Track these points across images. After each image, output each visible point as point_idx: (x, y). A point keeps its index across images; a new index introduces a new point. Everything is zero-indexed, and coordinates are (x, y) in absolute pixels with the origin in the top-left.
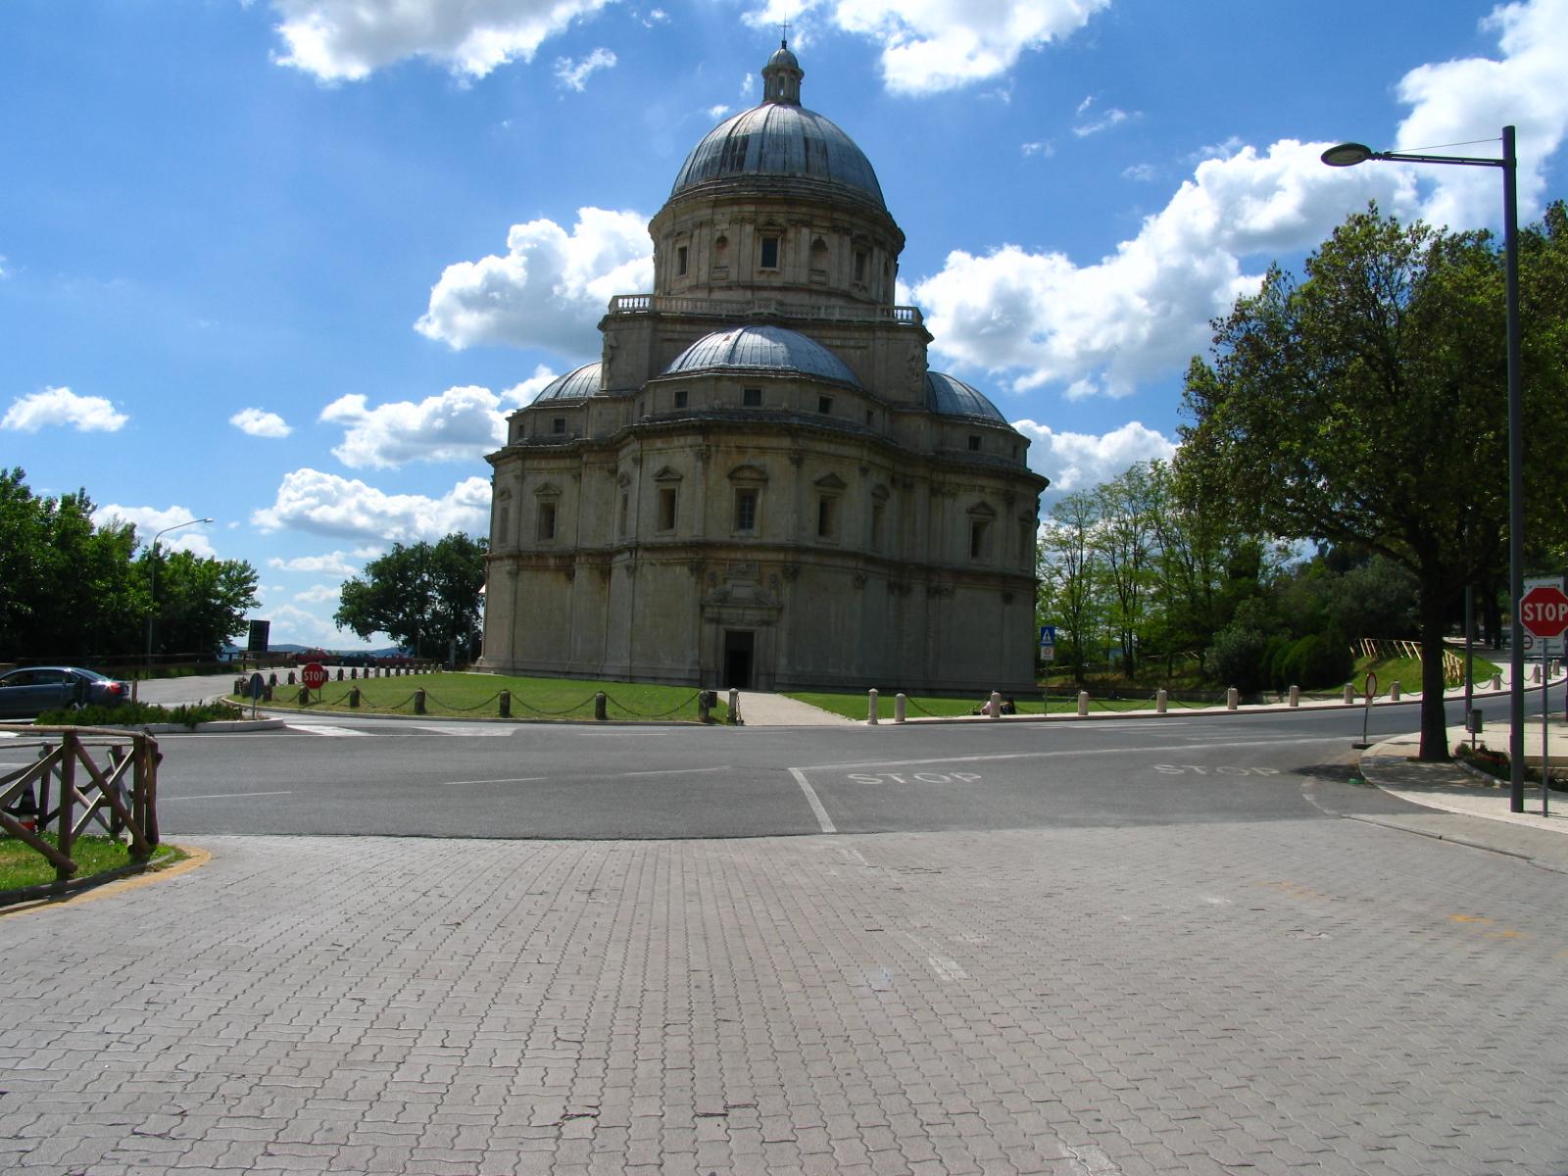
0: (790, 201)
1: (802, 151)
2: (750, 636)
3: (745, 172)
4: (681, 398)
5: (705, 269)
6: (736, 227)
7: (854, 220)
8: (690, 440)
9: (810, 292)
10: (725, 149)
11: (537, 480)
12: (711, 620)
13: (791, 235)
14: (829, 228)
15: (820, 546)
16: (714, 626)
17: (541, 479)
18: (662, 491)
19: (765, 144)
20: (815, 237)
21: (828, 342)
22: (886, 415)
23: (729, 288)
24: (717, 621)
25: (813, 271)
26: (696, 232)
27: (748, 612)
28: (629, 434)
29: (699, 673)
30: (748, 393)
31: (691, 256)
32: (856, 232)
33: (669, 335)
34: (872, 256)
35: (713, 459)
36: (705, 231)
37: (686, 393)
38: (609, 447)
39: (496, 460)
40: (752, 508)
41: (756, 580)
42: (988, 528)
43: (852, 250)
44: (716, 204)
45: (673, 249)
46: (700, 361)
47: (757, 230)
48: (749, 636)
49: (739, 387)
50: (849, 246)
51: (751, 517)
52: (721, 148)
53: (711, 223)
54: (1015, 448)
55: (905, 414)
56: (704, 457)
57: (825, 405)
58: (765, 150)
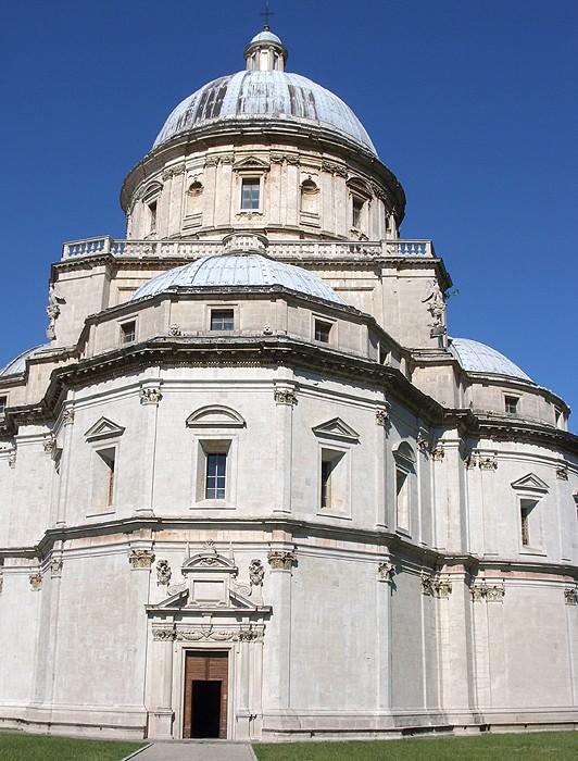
0: (270, 139)
1: (286, 94)
2: (223, 654)
3: (221, 117)
4: (128, 328)
12: (163, 635)
13: (276, 170)
16: (165, 644)
23: (204, 233)
27: (216, 620)
28: (59, 382)
30: (215, 314)
32: (350, 176)
33: (129, 284)
41: (231, 572)
44: (188, 150)
46: (154, 291)
48: (223, 654)
49: (204, 306)
51: (222, 483)
54: (557, 416)
55: (423, 365)
57: (323, 330)
58: (244, 96)
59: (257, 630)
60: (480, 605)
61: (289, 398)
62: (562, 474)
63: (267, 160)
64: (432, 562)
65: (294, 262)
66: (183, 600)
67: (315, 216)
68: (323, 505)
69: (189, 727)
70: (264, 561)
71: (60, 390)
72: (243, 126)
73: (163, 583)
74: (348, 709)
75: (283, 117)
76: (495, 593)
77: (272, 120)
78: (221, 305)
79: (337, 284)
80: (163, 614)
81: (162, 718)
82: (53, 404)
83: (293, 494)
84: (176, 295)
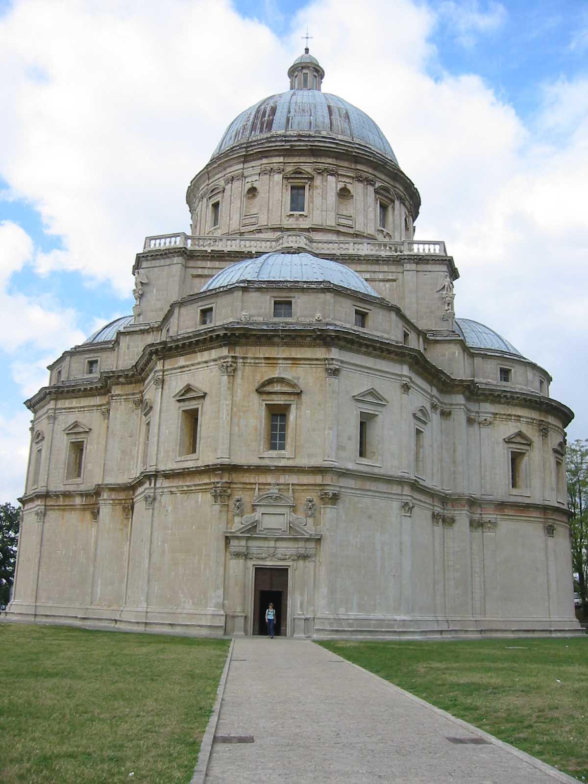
1: (326, 111)
2: (284, 571)
3: (273, 132)
4: (206, 313)
5: (236, 217)
7: (376, 173)
8: (214, 354)
9: (338, 233)
10: (256, 117)
11: (66, 420)
12: (237, 555)
13: (318, 181)
14: (353, 178)
15: (362, 468)
16: (241, 561)
17: (71, 419)
18: (185, 411)
19: (292, 110)
20: (341, 185)
22: (421, 339)
23: (259, 231)
24: (246, 556)
25: (339, 215)
26: (228, 187)
27: (280, 544)
28: (151, 354)
29: (223, 618)
31: (222, 208)
32: (377, 185)
33: (200, 272)
34: (393, 208)
35: (239, 373)
36: (237, 184)
37: (211, 309)
38: (137, 375)
39: (34, 405)
40: (283, 428)
42: (526, 458)
44: (246, 159)
45: (207, 206)
46: (227, 281)
47: (285, 178)
49: (268, 297)
50: (373, 195)
51: (283, 437)
52: (252, 117)
53: (243, 176)
54: (541, 382)
56: (230, 370)
58: (292, 114)
59: (312, 552)
60: (478, 534)
61: (335, 372)
63: (309, 170)
64: (445, 499)
65: (332, 257)
66: (254, 527)
67: (349, 217)
68: (362, 454)
69: (257, 627)
70: (316, 501)
71: (149, 360)
72: (291, 141)
73: (238, 515)
74: (379, 615)
75: (324, 133)
76: (489, 525)
77: (314, 137)
78: (283, 296)
79: (368, 276)
80: (238, 538)
81: (236, 619)
82: (143, 370)
83: (340, 448)
84: (246, 287)
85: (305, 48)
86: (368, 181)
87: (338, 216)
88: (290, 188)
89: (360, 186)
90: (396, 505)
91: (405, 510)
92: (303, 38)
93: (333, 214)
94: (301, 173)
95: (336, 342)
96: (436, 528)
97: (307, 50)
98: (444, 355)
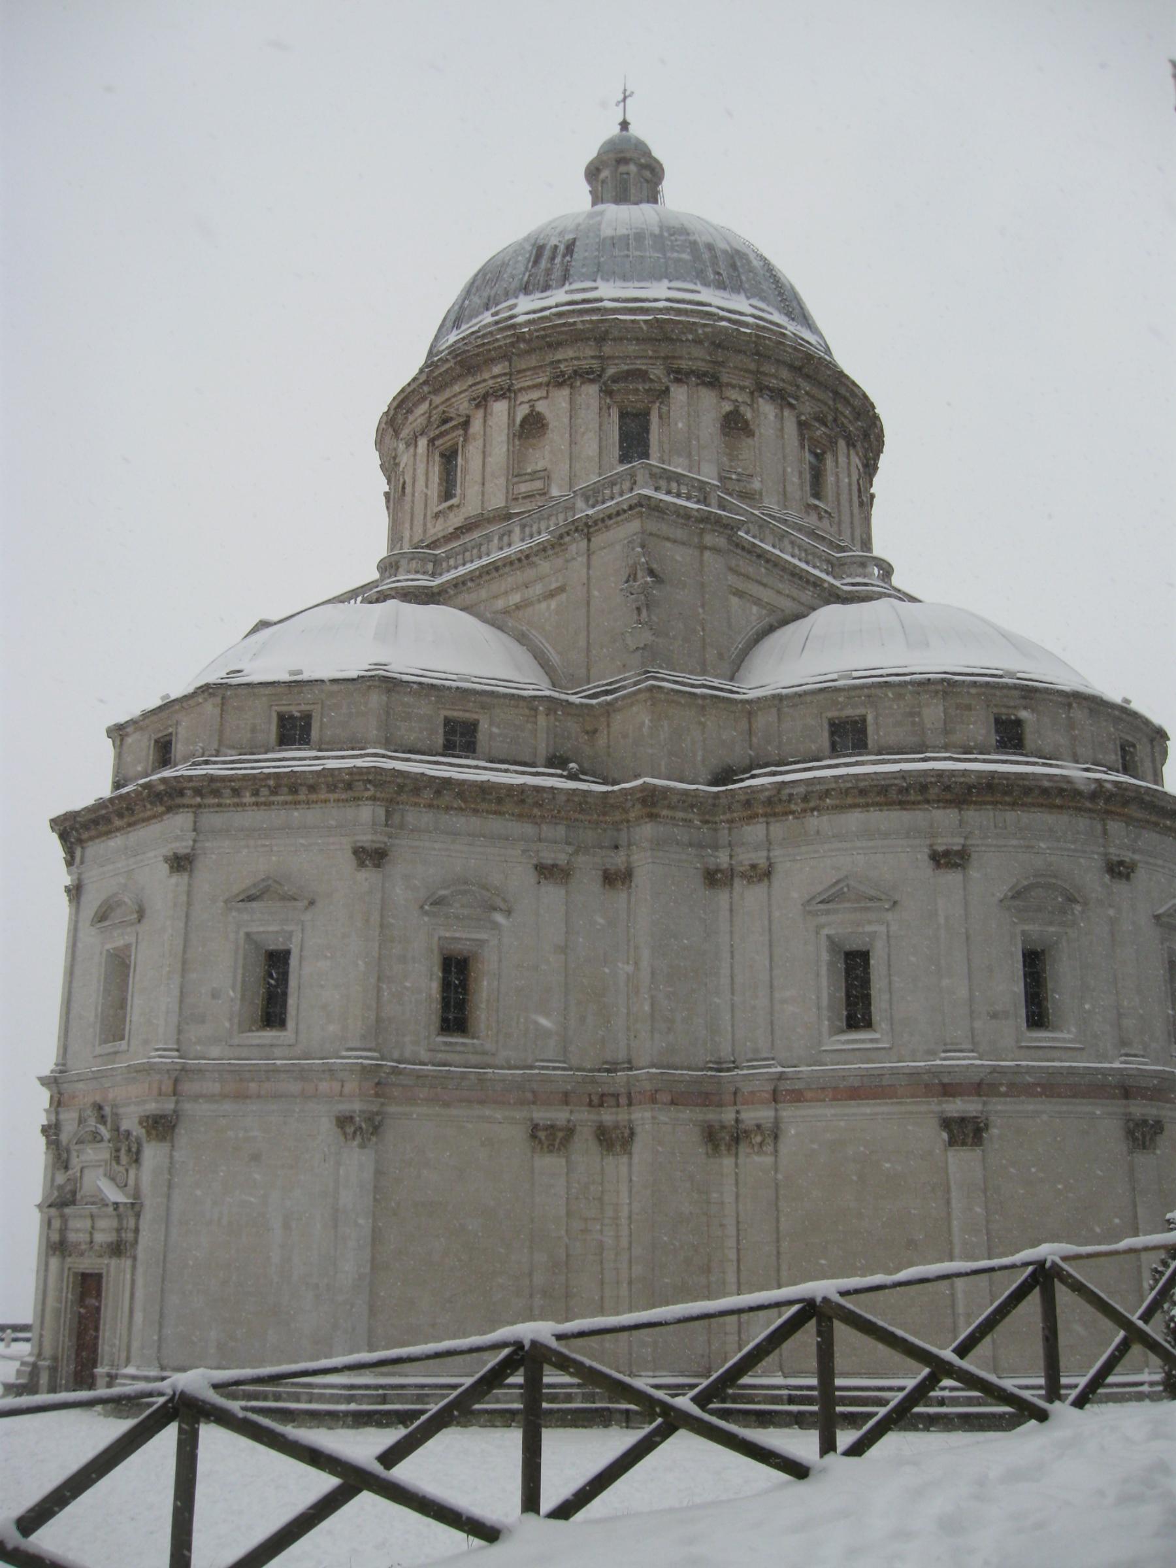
6: (412, 450)
14: (548, 384)
20: (522, 411)
21: (500, 604)
32: (611, 371)
43: (603, 410)
50: (595, 404)
59: (130, 1236)
61: (181, 863)
62: (947, 860)
85: (621, 120)
86: (581, 376)
87: (516, 479)
88: (437, 458)
89: (562, 396)
90: (327, 1125)
91: (345, 1134)
92: (618, 104)
93: (502, 481)
94: (451, 419)
95: (179, 801)
96: (549, 1163)
97: (624, 125)
98: (625, 736)
